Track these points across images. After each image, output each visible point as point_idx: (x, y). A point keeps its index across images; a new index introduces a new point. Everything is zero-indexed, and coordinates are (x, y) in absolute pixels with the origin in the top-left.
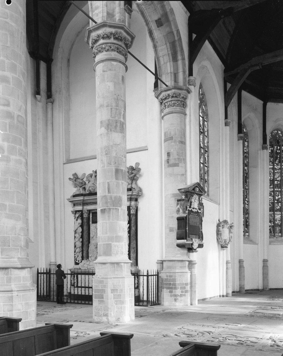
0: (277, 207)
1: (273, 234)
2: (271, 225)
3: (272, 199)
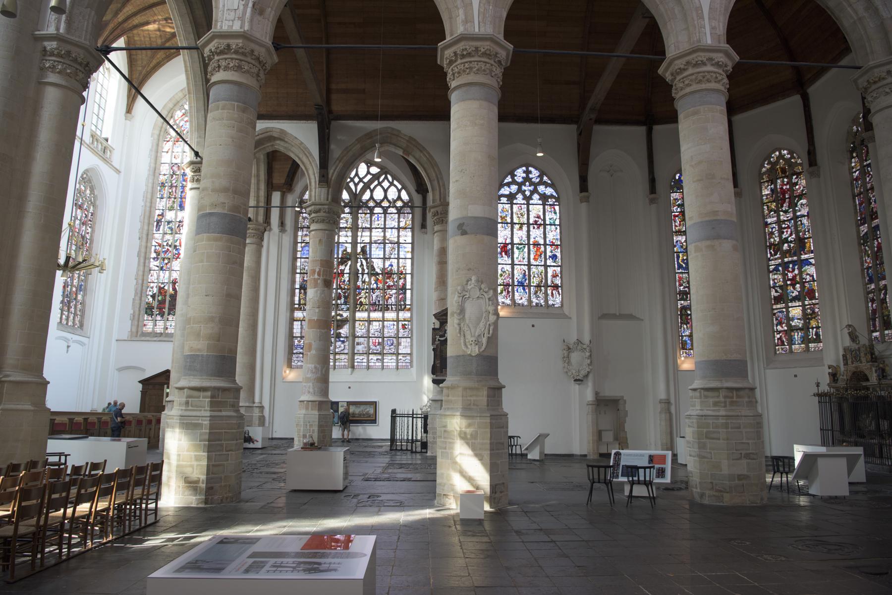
0: (793, 293)
1: (787, 347)
2: (782, 329)
3: (781, 280)
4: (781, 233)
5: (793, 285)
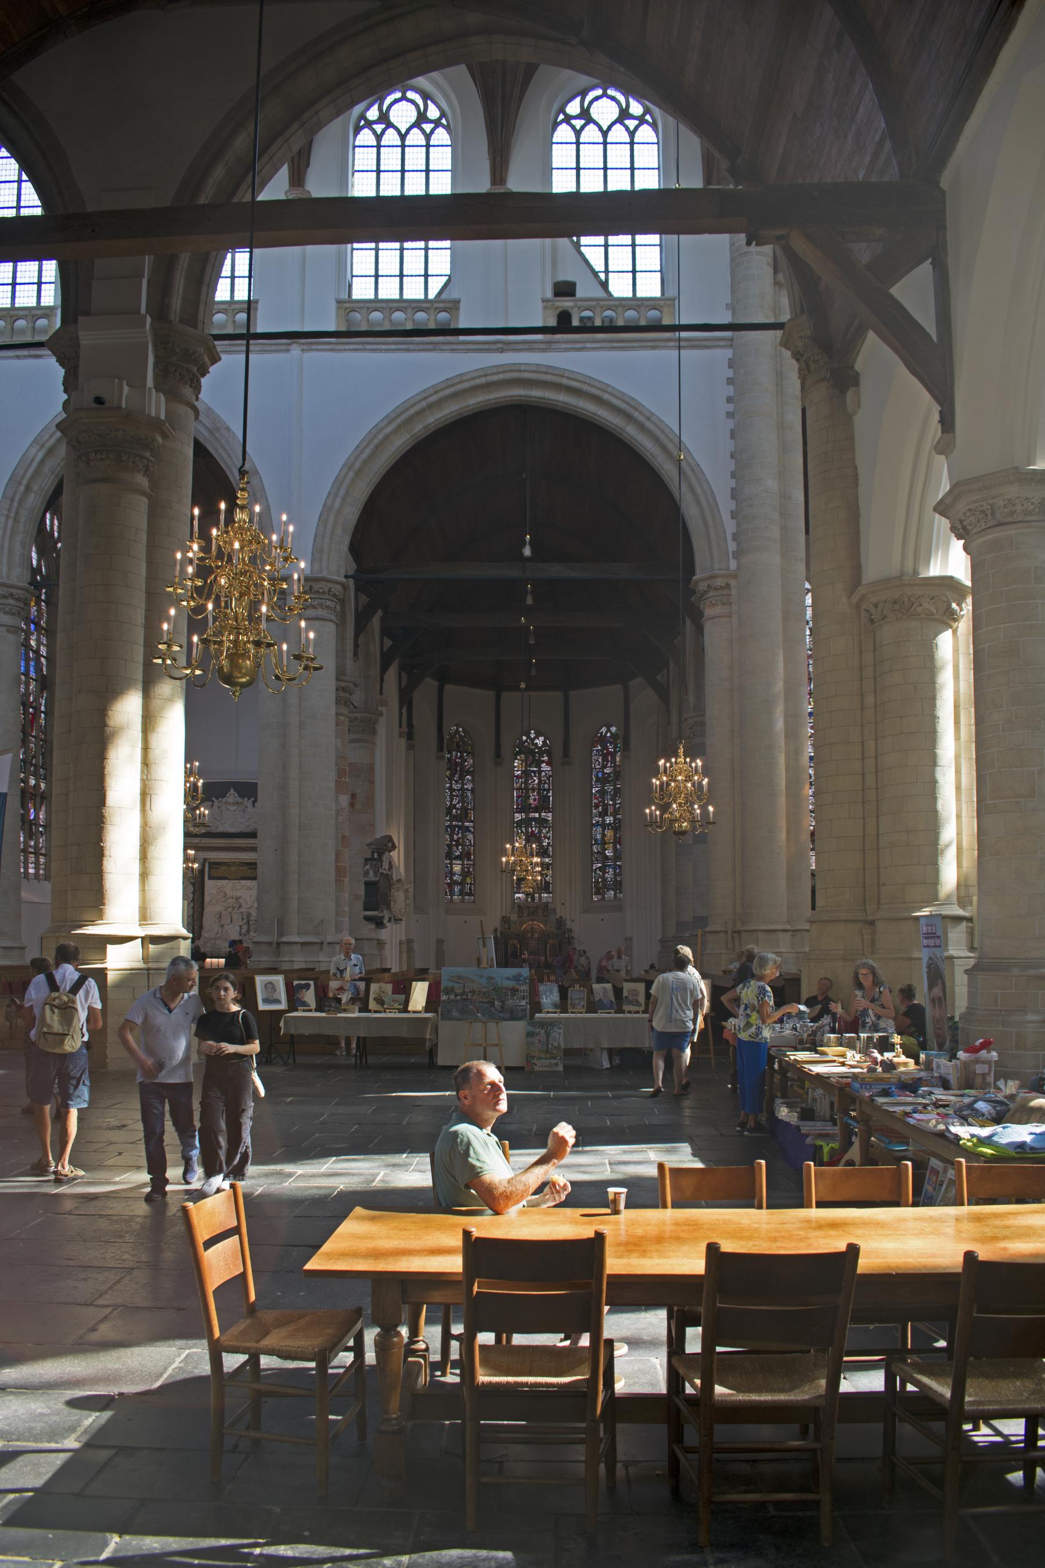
4: (451, 800)
5: (457, 846)
